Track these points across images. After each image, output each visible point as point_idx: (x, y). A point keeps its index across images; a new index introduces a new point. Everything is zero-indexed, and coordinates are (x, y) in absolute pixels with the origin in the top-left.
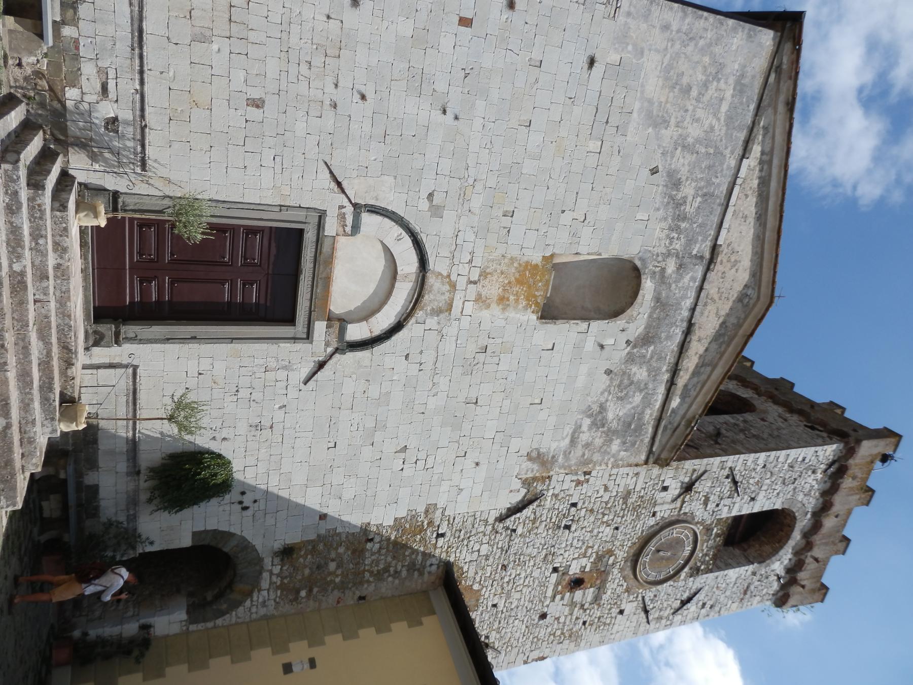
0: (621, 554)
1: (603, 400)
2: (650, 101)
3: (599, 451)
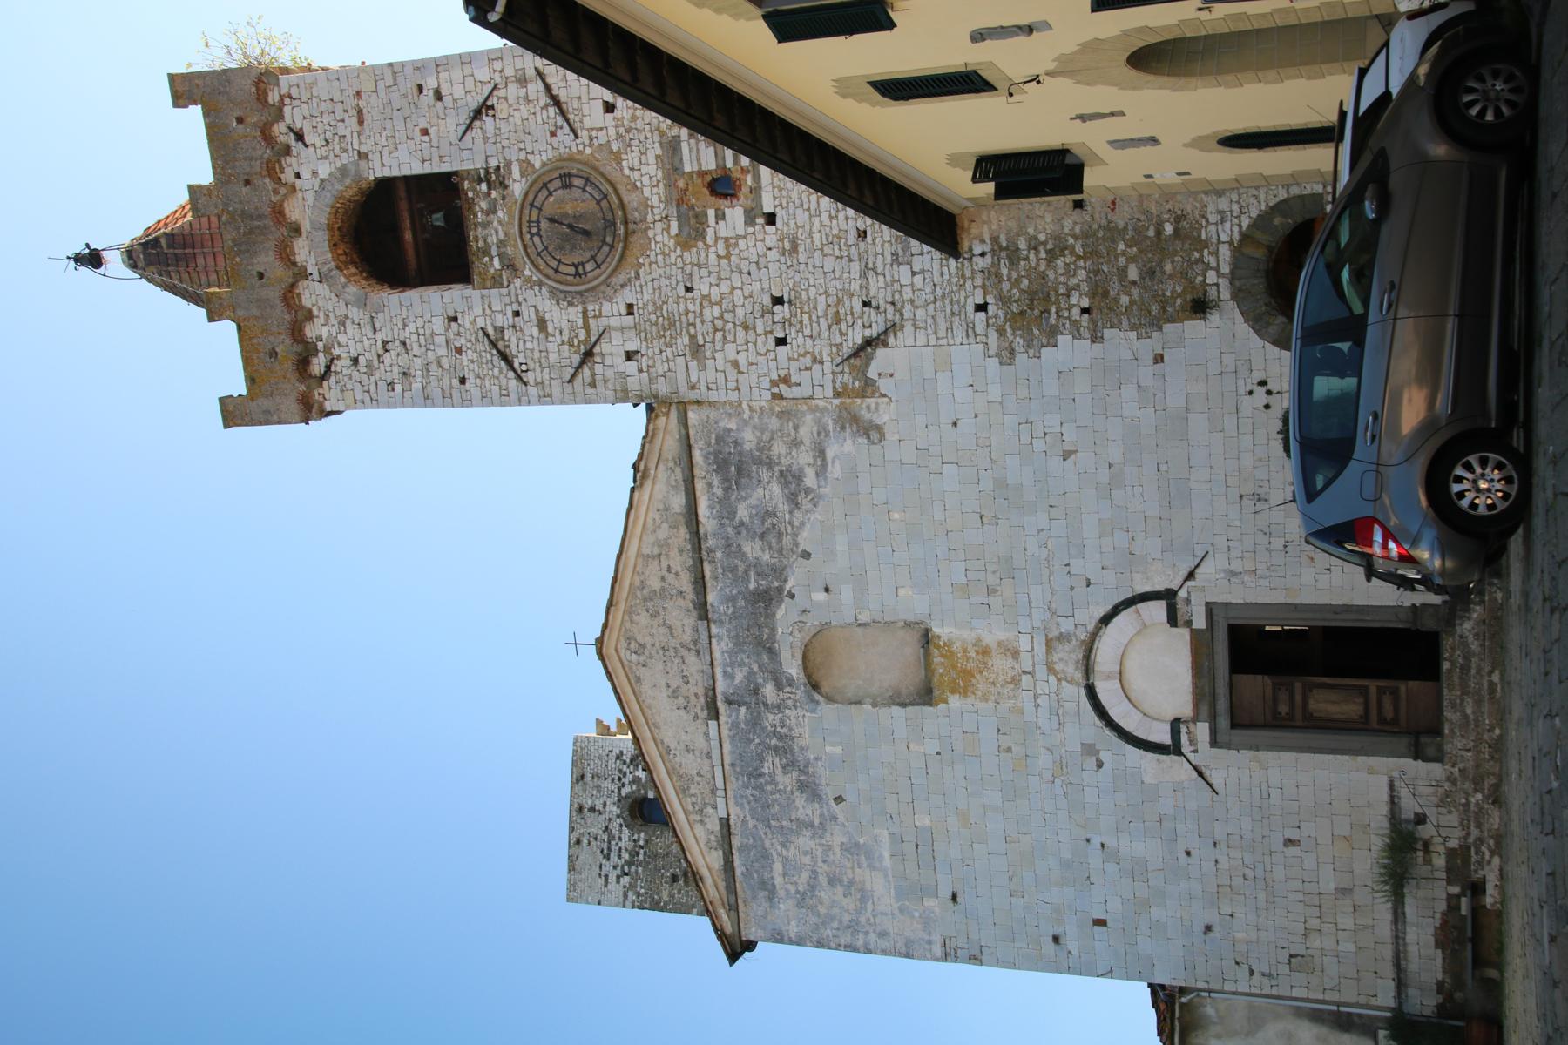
0: (661, 236)
1: (798, 514)
2: (872, 867)
3: (773, 433)
